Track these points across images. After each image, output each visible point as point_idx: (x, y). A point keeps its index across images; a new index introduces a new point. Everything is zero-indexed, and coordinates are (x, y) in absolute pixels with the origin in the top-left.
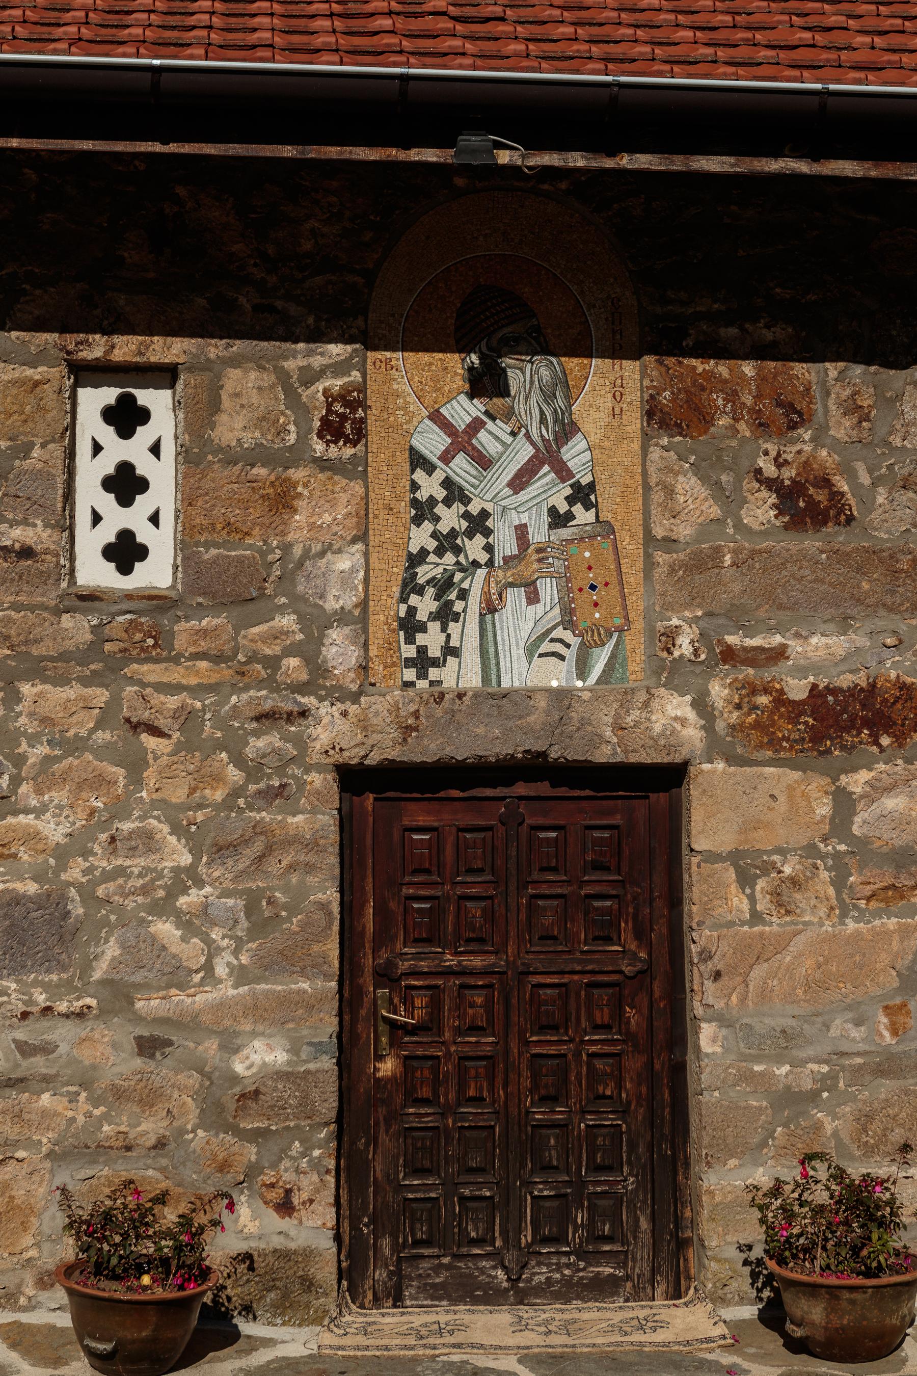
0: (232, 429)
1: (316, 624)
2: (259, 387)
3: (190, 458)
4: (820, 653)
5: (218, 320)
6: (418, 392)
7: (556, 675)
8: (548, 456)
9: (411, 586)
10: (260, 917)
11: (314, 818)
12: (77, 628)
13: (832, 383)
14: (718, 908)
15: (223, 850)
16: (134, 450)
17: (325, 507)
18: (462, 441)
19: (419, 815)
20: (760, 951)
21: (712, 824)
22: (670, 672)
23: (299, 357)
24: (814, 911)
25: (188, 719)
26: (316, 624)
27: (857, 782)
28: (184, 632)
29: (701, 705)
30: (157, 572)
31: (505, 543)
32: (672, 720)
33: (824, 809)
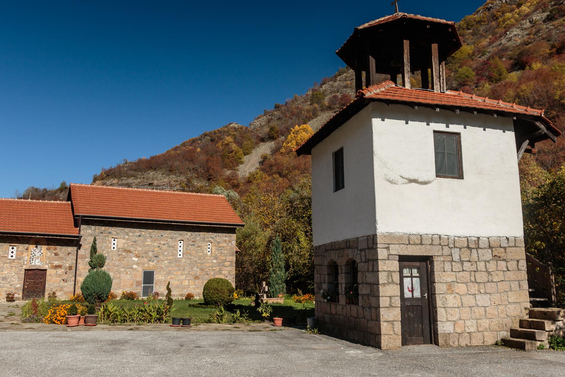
0: (20, 249)
1: (24, 261)
2: (22, 247)
3: (17, 251)
4: (56, 263)
6: (32, 247)
7: (39, 264)
8: (40, 251)
10: (19, 278)
11: (23, 272)
12: (9, 261)
13: (58, 247)
14: (48, 277)
16: (13, 250)
17: (25, 254)
18: (35, 250)
19: (30, 272)
20: (50, 280)
21: (48, 273)
22: (46, 264)
23: (24, 245)
24: (54, 278)
26: (24, 261)
30: (14, 258)
32: (46, 267)
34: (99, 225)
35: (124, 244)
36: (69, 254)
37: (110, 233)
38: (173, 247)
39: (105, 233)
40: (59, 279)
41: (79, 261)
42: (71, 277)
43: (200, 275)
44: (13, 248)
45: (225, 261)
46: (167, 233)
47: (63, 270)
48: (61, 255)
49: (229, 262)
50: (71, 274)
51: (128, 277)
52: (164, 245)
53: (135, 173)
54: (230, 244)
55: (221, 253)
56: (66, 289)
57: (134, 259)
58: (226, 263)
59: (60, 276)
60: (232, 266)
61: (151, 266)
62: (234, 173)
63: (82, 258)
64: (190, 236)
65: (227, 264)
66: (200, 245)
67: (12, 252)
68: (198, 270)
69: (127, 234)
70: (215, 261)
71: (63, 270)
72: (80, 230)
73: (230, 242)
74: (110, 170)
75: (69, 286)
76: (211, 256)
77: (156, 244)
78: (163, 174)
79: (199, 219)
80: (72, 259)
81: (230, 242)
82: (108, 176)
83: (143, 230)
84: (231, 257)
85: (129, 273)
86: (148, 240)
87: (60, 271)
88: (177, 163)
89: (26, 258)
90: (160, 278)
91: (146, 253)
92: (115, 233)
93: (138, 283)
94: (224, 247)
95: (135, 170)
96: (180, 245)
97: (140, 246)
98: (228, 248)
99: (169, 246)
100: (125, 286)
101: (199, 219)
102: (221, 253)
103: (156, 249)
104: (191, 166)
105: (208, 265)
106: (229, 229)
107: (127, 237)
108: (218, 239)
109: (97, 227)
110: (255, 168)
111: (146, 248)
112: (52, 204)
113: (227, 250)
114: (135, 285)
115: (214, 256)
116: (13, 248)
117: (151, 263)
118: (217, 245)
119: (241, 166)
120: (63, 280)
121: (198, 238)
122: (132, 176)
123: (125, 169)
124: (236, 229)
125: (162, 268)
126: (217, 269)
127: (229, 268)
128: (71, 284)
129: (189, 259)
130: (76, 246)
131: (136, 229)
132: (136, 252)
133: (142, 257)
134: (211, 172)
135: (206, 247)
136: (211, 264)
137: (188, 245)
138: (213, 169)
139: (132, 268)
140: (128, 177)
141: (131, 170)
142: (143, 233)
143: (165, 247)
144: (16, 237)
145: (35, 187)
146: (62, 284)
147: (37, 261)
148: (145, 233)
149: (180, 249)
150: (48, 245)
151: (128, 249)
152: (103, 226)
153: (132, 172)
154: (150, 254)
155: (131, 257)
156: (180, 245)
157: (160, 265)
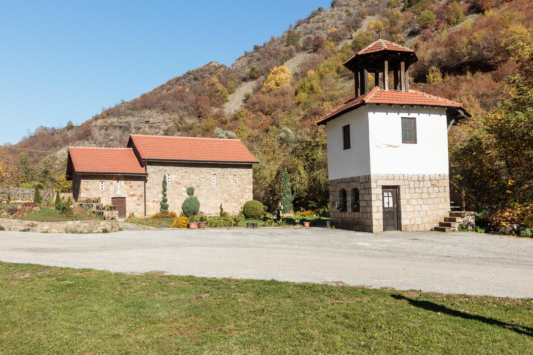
3: (105, 185)
4: (132, 193)
5: (106, 179)
6: (115, 182)
11: (111, 199)
13: (132, 182)
14: (127, 203)
17: (111, 187)
21: (127, 199)
22: (125, 193)
32: (125, 196)
36: (139, 186)
38: (209, 179)
45: (246, 188)
46: (204, 170)
48: (134, 187)
53: (133, 112)
56: (139, 211)
57: (183, 188)
59: (135, 201)
62: (221, 111)
65: (247, 190)
66: (227, 177)
70: (238, 189)
72: (146, 169)
73: (248, 174)
74: (110, 110)
77: (197, 178)
78: (157, 112)
81: (248, 174)
82: (108, 115)
83: (188, 168)
84: (250, 186)
87: (135, 198)
88: (169, 102)
89: (112, 190)
94: (244, 178)
95: (132, 109)
99: (206, 179)
102: (243, 183)
104: (182, 105)
105: (234, 192)
106: (248, 166)
108: (240, 173)
110: (239, 105)
112: (120, 150)
119: (226, 104)
121: (226, 173)
122: (130, 115)
123: (123, 108)
125: (202, 195)
126: (240, 194)
127: (249, 194)
134: (201, 110)
138: (202, 108)
139: (182, 195)
140: (127, 115)
141: (128, 109)
143: (204, 180)
144: (104, 176)
145: (44, 126)
146: (137, 207)
150: (125, 180)
151: (178, 182)
153: (129, 111)
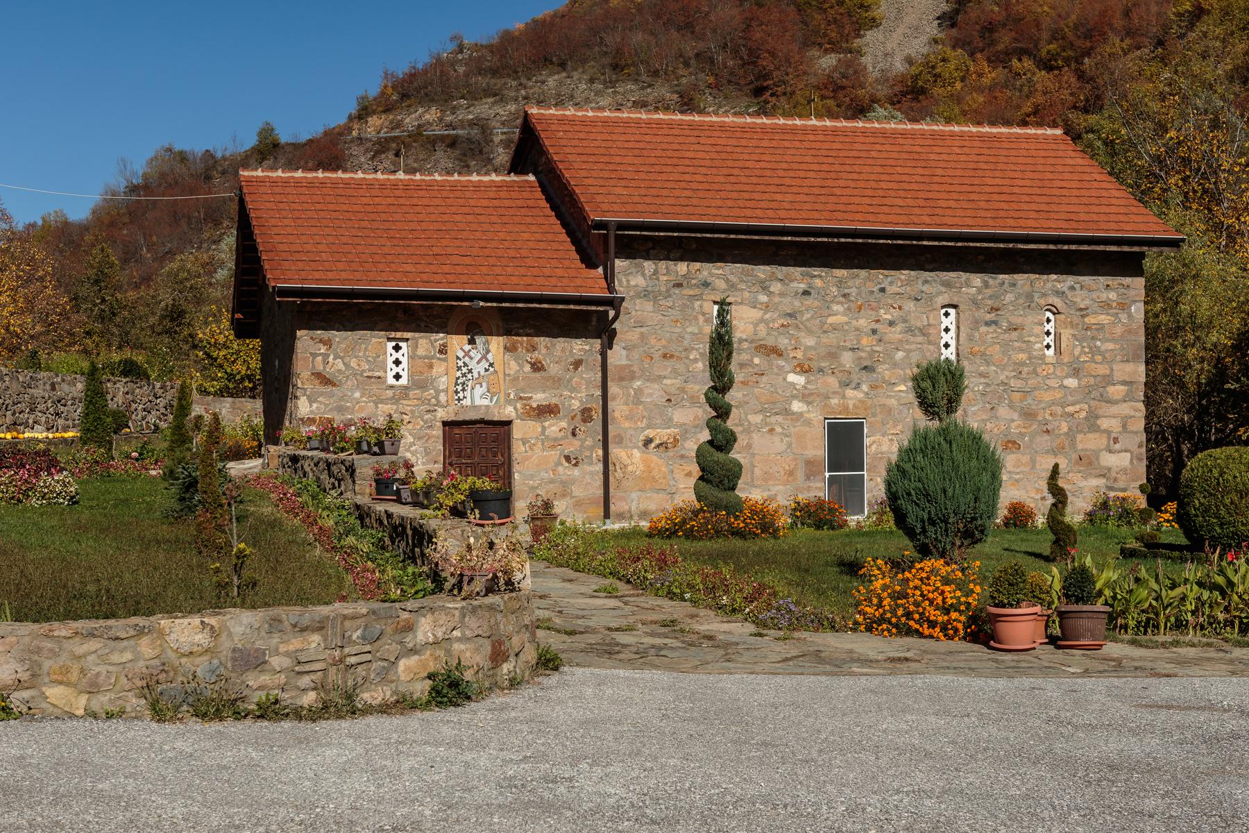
0: (421, 352)
1: (438, 392)
2: (426, 343)
3: (412, 357)
4: (539, 398)
5: (418, 329)
6: (458, 343)
7: (486, 402)
8: (484, 357)
9: (457, 384)
10: (427, 452)
11: (438, 432)
12: (390, 393)
13: (542, 341)
14: (518, 450)
15: (419, 438)
16: (398, 355)
17: (439, 368)
18: (467, 354)
19: (457, 431)
20: (527, 458)
21: (517, 432)
22: (509, 402)
23: (434, 336)
24: (538, 449)
25: (412, 412)
26: (438, 392)
27: (546, 424)
28: (411, 393)
29: (515, 408)
30: (404, 381)
31: (476, 375)
32: (509, 412)
33: (540, 429)
34: (668, 258)
35: (756, 325)
36: (577, 364)
37: (706, 284)
38: (923, 332)
39: (690, 286)
40: (555, 454)
41: (613, 389)
42: (592, 448)
43: (1022, 435)
44: (397, 348)
45: (1108, 380)
46: (898, 281)
47: (564, 424)
48: (553, 369)
49: (1124, 383)
50: (590, 438)
51: (778, 444)
52: (891, 324)
53: (497, 82)
54: (1124, 317)
55: (1094, 351)
56: (578, 491)
57: (792, 378)
58: (1111, 389)
59: (555, 443)
60: (1133, 400)
61: (852, 402)
62: (849, 64)
63: (622, 379)
64: (979, 291)
65: (1117, 391)
66: (1017, 320)
67: (397, 362)
68: (1015, 416)
69: (765, 289)
70: (1072, 382)
71: (564, 424)
72: (609, 278)
73: (1123, 306)
74: (412, 76)
75: (588, 479)
76: (1059, 363)
77: (862, 322)
78: (592, 81)
79: (1012, 222)
80: (589, 382)
81: (1123, 306)
82: (404, 96)
83: (816, 271)
84: (1129, 367)
85: (779, 429)
86: (835, 307)
87: (554, 427)
88: (638, 37)
89: (443, 382)
90: (885, 448)
91: (833, 355)
92: (721, 284)
93: (811, 468)
94: (1101, 327)
95: (495, 72)
96: (946, 322)
97: (810, 332)
98: (1119, 330)
99: (909, 330)
100: (767, 477)
101: (1012, 222)
102: (1094, 351)
103: (864, 341)
104: (690, 47)
105: (1047, 397)
106: (1114, 259)
107: (763, 298)
108: (1081, 299)
109: (663, 265)
110: (924, 39)
111: (831, 339)
112: (477, 186)
113: (1113, 340)
114: (800, 474)
115: (1070, 364)
116: (397, 348)
117: (850, 392)
118: (1076, 320)
119: (870, 36)
120: (568, 458)
121: (1009, 297)
122: (488, 92)
123: (461, 70)
124: (1142, 255)
125: (888, 411)
126: (1081, 410)
127: (1125, 409)
128: (591, 473)
129: (982, 375)
130: (599, 337)
131: (791, 269)
132: (799, 354)
133: (821, 370)
134: (766, 62)
135: (1037, 329)
136: (1058, 395)
137: (976, 323)
138: (773, 54)
139: (787, 412)
140: (474, 96)
141: (480, 71)
142: (818, 283)
143: (895, 334)
144: (407, 310)
145: (178, 147)
146: (565, 471)
147: (479, 391)
148: (825, 279)
149: (946, 338)
150: (508, 332)
151: (770, 342)
152: (682, 259)
153: (482, 81)
154: (847, 359)
155: (782, 372)
156: (946, 322)
157: (883, 401)
